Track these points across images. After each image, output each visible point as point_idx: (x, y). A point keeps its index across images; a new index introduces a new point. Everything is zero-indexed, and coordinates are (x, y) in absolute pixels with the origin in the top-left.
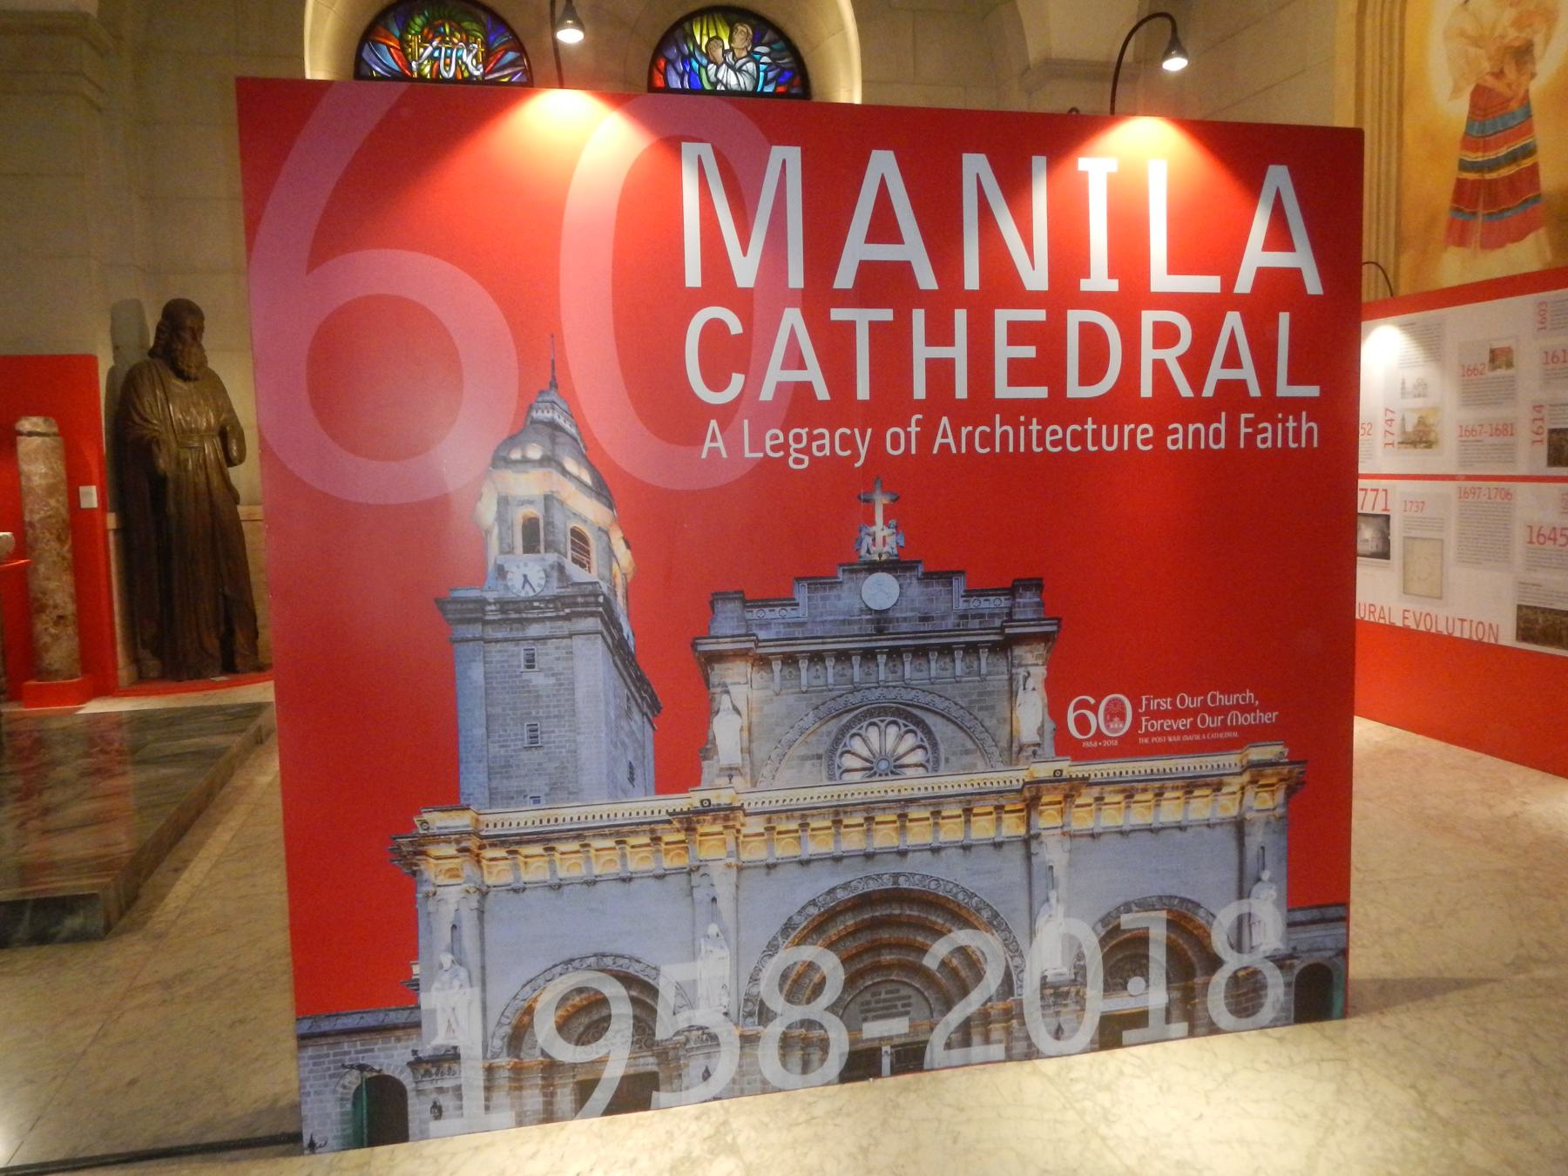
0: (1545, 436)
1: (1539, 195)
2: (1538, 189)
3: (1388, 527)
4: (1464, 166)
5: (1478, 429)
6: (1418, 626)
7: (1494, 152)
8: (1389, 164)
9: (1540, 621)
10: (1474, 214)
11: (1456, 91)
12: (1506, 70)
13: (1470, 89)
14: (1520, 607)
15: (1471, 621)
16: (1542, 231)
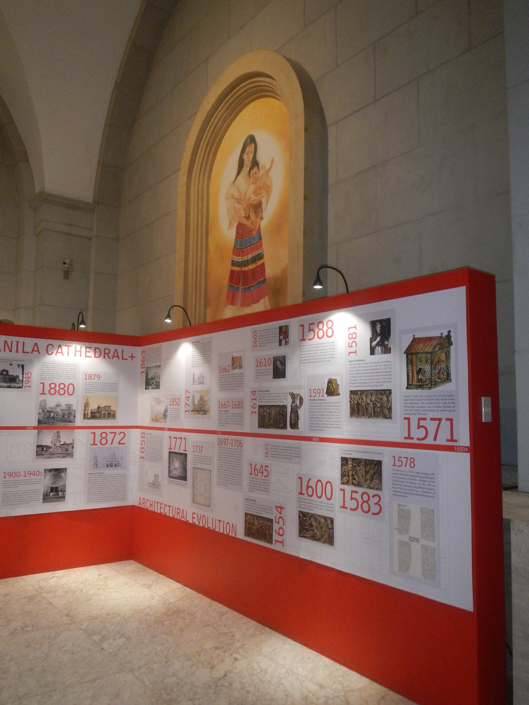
0: (257, 409)
1: (265, 280)
2: (265, 276)
3: (186, 462)
4: (234, 264)
5: (227, 403)
6: (199, 524)
7: (246, 257)
8: (201, 260)
9: (256, 524)
10: (238, 288)
11: (230, 225)
12: (251, 216)
13: (236, 224)
14: (246, 514)
15: (224, 522)
16: (267, 298)
